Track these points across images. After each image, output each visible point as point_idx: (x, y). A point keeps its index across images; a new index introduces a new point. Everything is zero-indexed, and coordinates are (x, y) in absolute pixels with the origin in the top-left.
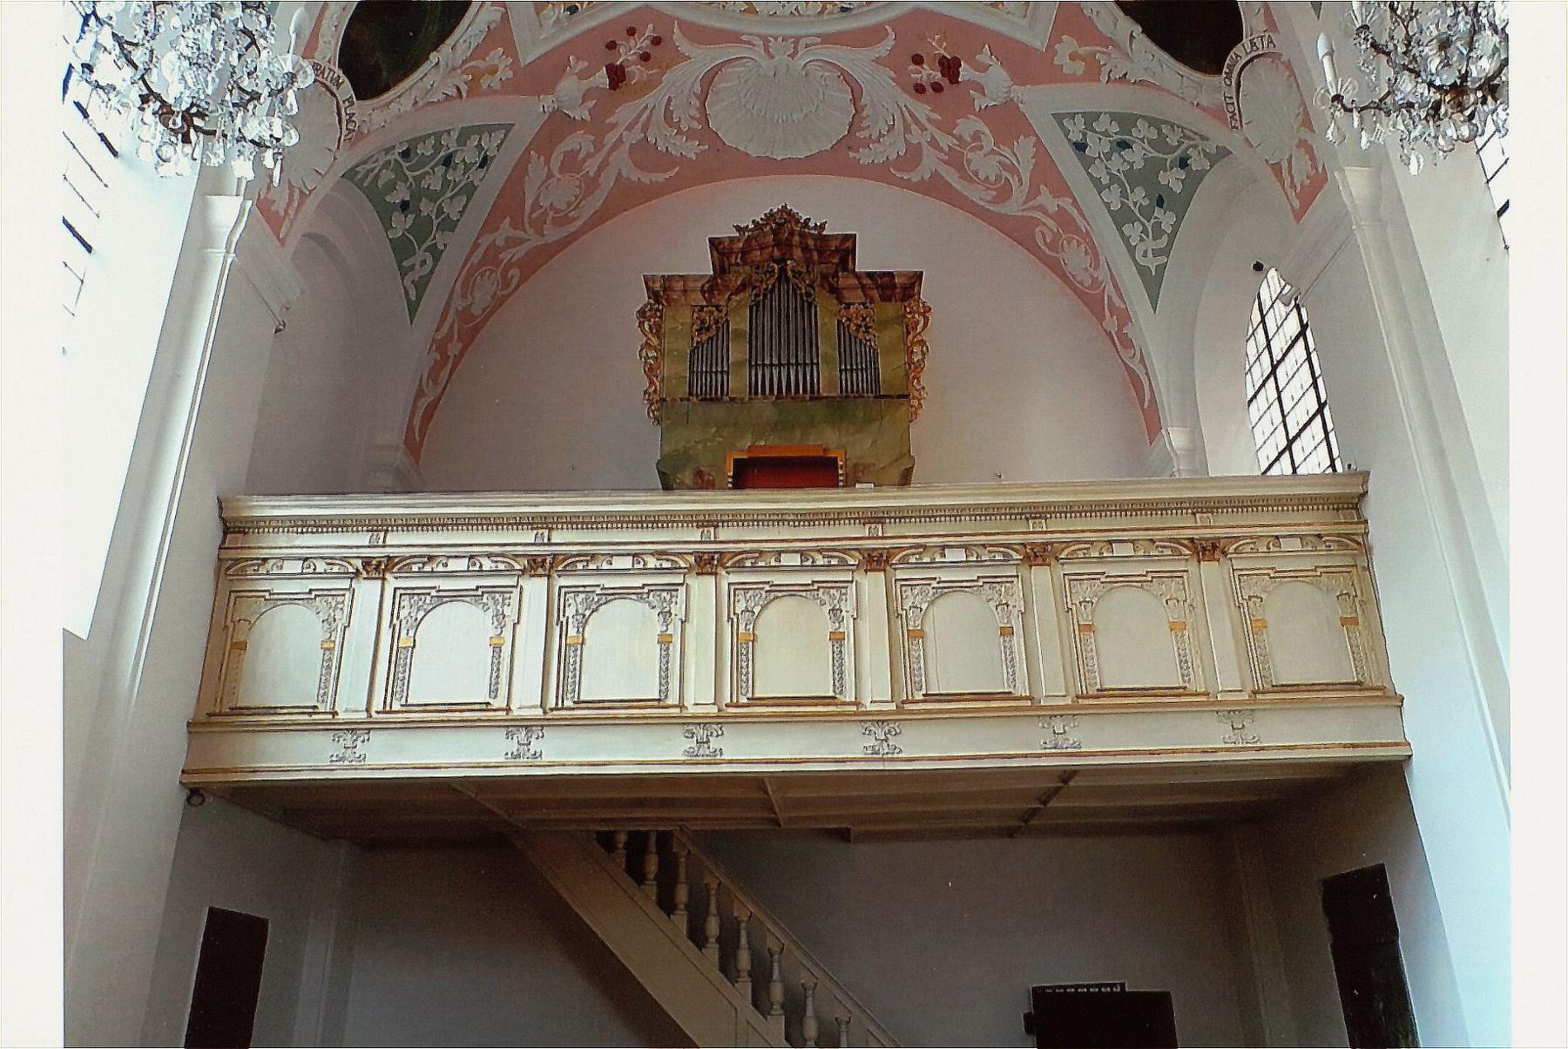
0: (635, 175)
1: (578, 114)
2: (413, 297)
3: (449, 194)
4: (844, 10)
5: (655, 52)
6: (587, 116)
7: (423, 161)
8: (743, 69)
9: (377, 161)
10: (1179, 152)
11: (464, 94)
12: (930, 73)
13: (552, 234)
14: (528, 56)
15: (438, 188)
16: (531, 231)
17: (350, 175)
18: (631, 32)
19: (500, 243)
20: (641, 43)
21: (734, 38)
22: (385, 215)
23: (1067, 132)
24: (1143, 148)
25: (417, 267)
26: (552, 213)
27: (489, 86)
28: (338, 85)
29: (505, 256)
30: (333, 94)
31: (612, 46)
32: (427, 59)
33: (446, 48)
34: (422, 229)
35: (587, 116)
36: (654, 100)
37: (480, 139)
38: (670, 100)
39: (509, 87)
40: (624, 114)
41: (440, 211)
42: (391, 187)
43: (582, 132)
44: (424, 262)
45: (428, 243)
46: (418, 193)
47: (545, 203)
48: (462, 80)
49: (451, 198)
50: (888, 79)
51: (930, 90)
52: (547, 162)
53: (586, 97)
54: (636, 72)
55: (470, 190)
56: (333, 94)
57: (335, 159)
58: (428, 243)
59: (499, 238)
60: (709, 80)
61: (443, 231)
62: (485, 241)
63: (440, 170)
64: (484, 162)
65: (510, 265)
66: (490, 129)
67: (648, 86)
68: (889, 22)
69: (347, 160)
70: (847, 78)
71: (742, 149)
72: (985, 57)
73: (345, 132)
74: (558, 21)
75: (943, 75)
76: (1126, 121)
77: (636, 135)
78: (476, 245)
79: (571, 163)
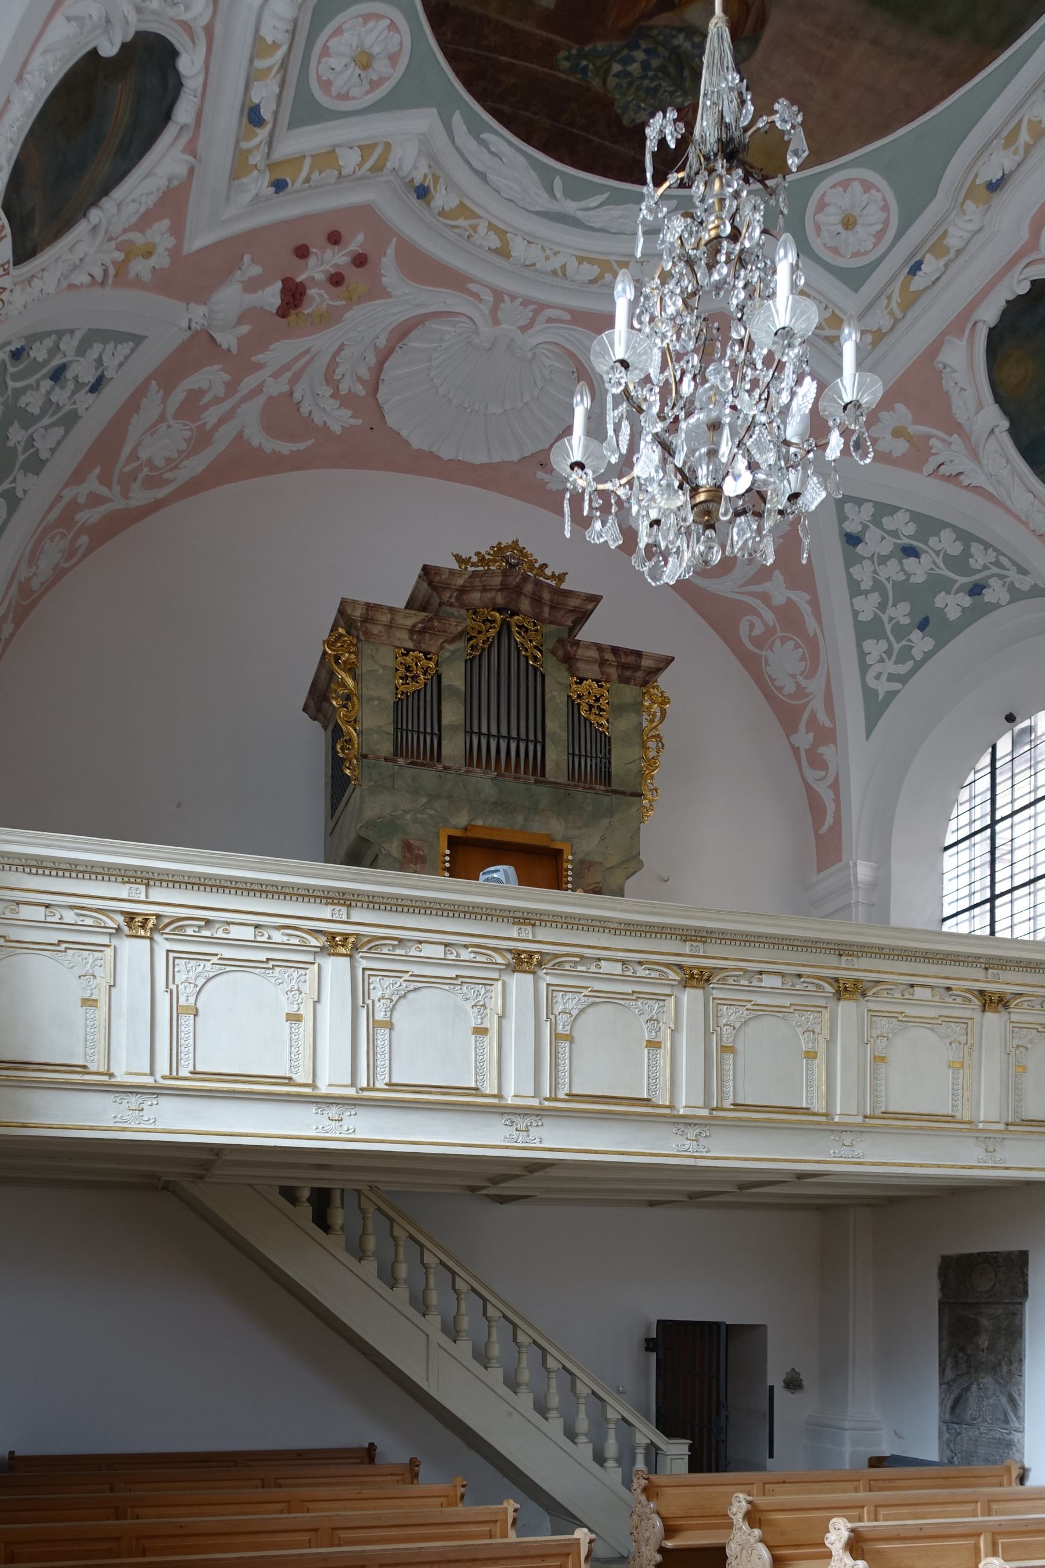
5: (353, 276)
7: (36, 366)
8: (452, 329)
13: (139, 497)
16: (117, 488)
26: (146, 470)
36: (323, 342)
38: (341, 348)
43: (221, 366)
47: (143, 455)
54: (318, 297)
55: (70, 420)
60: (403, 332)
63: (47, 384)
67: (328, 319)
71: (404, 433)
77: (280, 387)
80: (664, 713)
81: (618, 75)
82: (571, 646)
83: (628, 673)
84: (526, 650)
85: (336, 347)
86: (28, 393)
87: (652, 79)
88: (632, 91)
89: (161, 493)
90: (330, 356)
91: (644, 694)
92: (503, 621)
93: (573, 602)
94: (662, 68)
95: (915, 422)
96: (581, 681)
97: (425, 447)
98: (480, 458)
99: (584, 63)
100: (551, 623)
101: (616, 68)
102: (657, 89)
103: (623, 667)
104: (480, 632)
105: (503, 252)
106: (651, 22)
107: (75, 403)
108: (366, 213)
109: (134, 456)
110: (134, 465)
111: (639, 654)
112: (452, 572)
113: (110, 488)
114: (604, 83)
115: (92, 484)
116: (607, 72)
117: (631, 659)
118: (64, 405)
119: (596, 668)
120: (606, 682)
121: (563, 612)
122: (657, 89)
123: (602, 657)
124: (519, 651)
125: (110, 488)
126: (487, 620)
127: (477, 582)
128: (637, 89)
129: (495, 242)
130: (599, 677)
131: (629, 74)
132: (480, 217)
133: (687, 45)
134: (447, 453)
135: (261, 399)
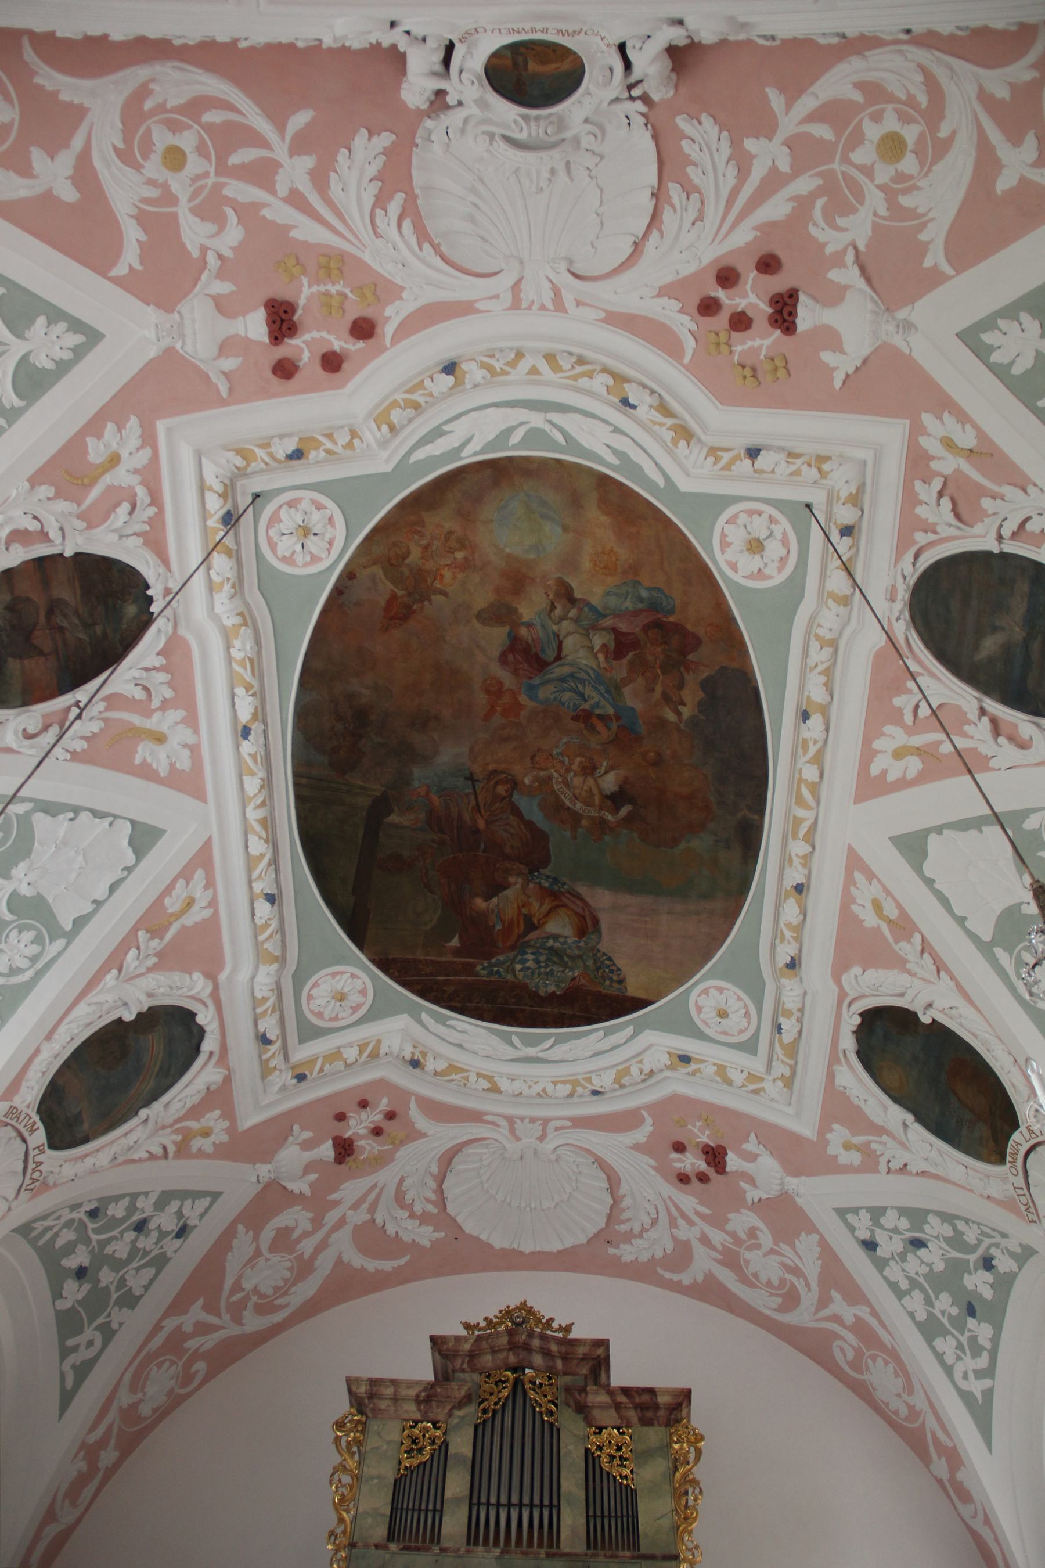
0: (357, 1260)
1: (295, 1187)
2: (69, 1383)
3: (135, 1264)
4: (595, 1093)
6: (307, 1191)
7: (115, 1222)
9: (59, 1218)
10: (981, 1251)
11: (171, 1155)
12: (692, 1162)
13: (253, 1323)
14: (249, 1120)
15: (124, 1256)
16: (226, 1317)
17: (24, 1230)
18: (364, 1104)
19: (188, 1328)
20: (373, 1117)
21: (476, 1117)
22: (56, 1278)
23: (852, 1229)
24: (941, 1248)
25: (82, 1347)
26: (254, 1299)
27: (200, 1149)
28: (32, 1131)
29: (192, 1344)
30: (24, 1140)
31: (341, 1117)
32: (136, 1114)
33: (157, 1106)
34: (96, 1302)
35: (307, 1191)
36: (387, 1177)
37: (182, 1205)
38: (402, 1180)
39: (227, 1152)
40: (350, 1190)
41: (122, 1282)
42: (69, 1249)
44: (90, 1343)
45: (101, 1320)
46: (101, 1259)
47: (248, 1285)
48: (169, 1139)
49: (138, 1269)
50: (646, 1167)
51: (694, 1180)
52: (256, 1238)
53: (308, 1169)
54: (367, 1146)
55: (160, 1262)
56: (24, 1140)
57: (9, 1209)
58: (101, 1320)
59: (188, 1321)
60: (448, 1159)
61: (120, 1309)
62: (170, 1324)
63: (131, 1235)
64: (182, 1232)
65: (196, 1356)
66: (195, 1195)
67: (381, 1161)
68: (648, 1107)
69: (26, 1210)
70: (601, 1164)
72: (751, 1145)
73: (28, 1181)
74: (284, 1088)
75: (708, 1164)
76: (917, 1216)
77: (360, 1217)
78: (157, 1328)
79: (284, 1240)
80: (699, 1453)
81: (521, 970)
82: (580, 1394)
83: (649, 1414)
84: (541, 1406)
85: (397, 1179)
86: (113, 1243)
87: (546, 967)
88: (536, 975)
89: (278, 1318)
90: (394, 1188)
91: (671, 1434)
92: (516, 1380)
93: (581, 1350)
94: (548, 960)
95: (853, 1135)
96: (600, 1430)
97: (506, 1245)
98: (555, 1246)
99: (495, 969)
100: (565, 1374)
101: (518, 967)
102: (552, 971)
103: (640, 1407)
104: (492, 1394)
105: (495, 1089)
106: (527, 938)
107: (162, 1247)
108: (382, 1085)
109: (237, 1287)
110: (239, 1295)
111: (651, 1391)
112: (458, 1339)
113: (219, 1315)
114: (515, 975)
115: (196, 1313)
116: (513, 970)
117: (646, 1398)
118: (151, 1251)
119: (613, 1412)
120: (627, 1427)
121: (575, 1362)
122: (552, 971)
123: (614, 1401)
124: (534, 1408)
125: (219, 1315)
126: (500, 1381)
127: (484, 1345)
128: (539, 974)
129: (485, 1084)
130: (618, 1423)
131: (529, 968)
132: (467, 1071)
133: (557, 944)
134: (527, 1247)
135: (346, 1232)
